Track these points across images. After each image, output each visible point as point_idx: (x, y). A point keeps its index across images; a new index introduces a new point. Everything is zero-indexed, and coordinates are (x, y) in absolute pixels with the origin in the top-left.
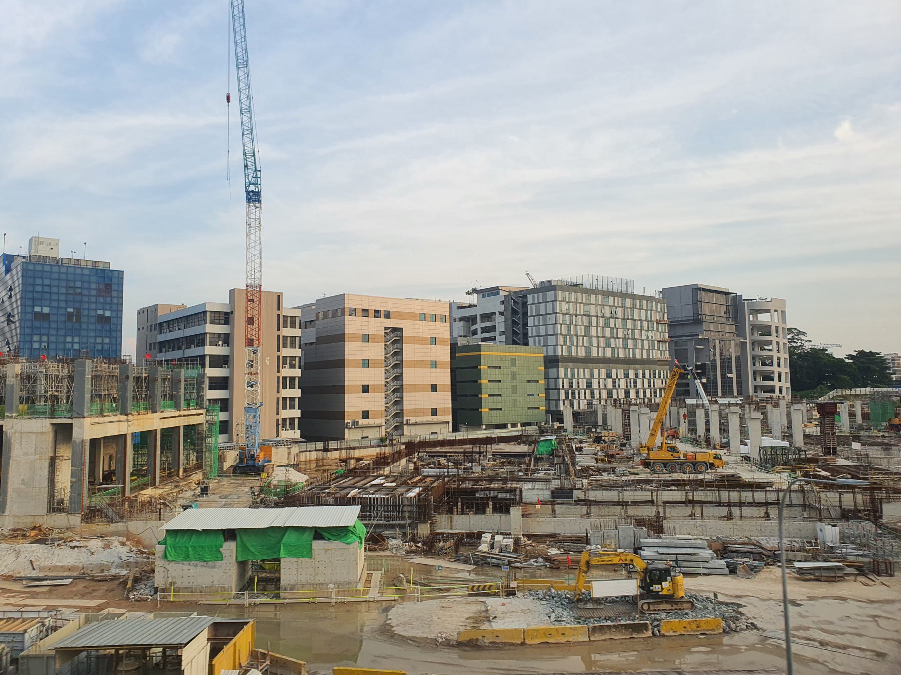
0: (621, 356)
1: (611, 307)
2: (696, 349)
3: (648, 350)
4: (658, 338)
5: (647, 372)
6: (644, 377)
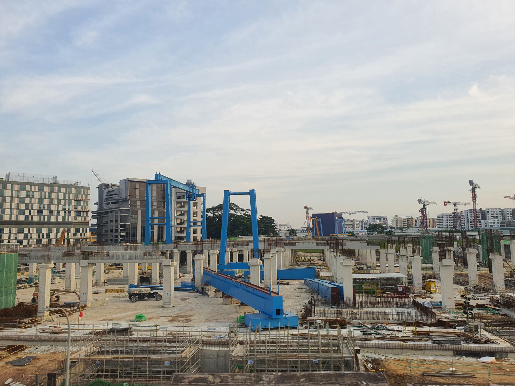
0: (35, 219)
1: (27, 192)
2: (121, 216)
3: (64, 218)
4: (79, 208)
5: (61, 230)
6: (58, 231)
